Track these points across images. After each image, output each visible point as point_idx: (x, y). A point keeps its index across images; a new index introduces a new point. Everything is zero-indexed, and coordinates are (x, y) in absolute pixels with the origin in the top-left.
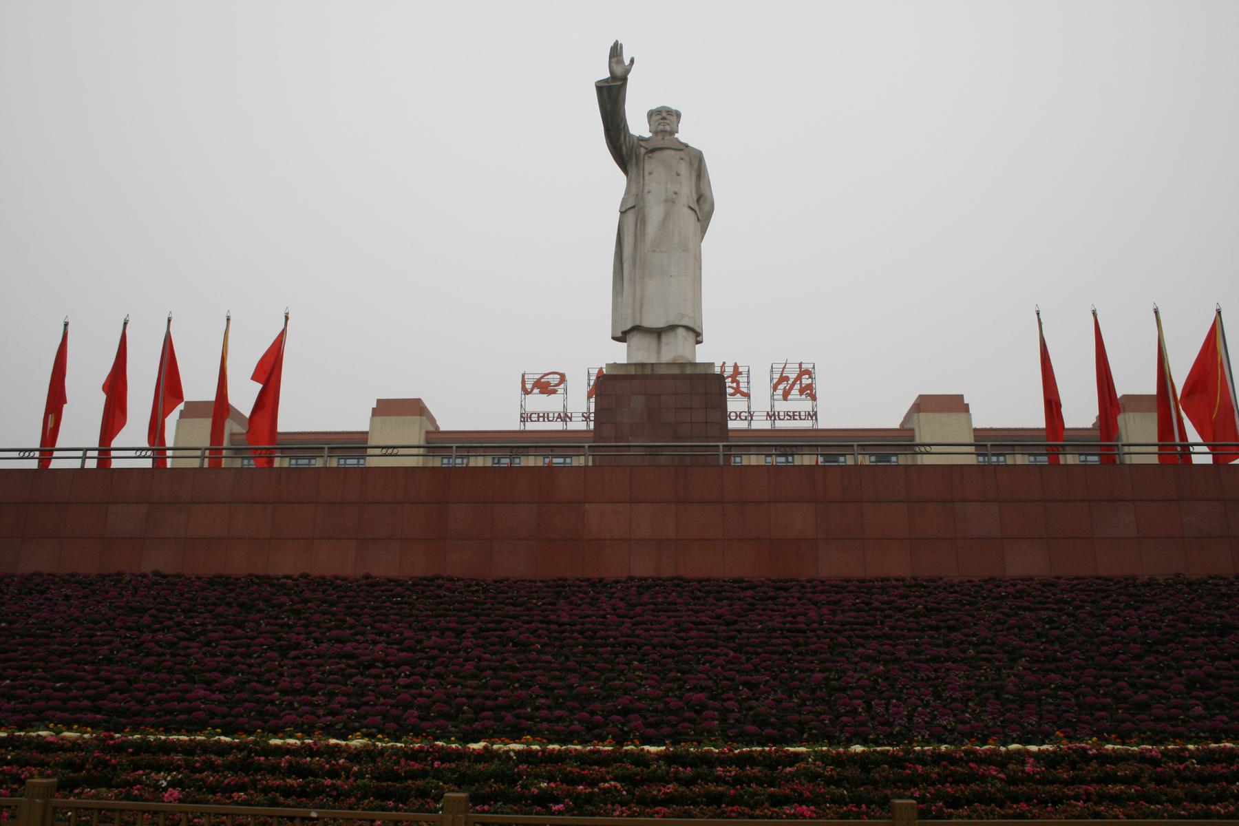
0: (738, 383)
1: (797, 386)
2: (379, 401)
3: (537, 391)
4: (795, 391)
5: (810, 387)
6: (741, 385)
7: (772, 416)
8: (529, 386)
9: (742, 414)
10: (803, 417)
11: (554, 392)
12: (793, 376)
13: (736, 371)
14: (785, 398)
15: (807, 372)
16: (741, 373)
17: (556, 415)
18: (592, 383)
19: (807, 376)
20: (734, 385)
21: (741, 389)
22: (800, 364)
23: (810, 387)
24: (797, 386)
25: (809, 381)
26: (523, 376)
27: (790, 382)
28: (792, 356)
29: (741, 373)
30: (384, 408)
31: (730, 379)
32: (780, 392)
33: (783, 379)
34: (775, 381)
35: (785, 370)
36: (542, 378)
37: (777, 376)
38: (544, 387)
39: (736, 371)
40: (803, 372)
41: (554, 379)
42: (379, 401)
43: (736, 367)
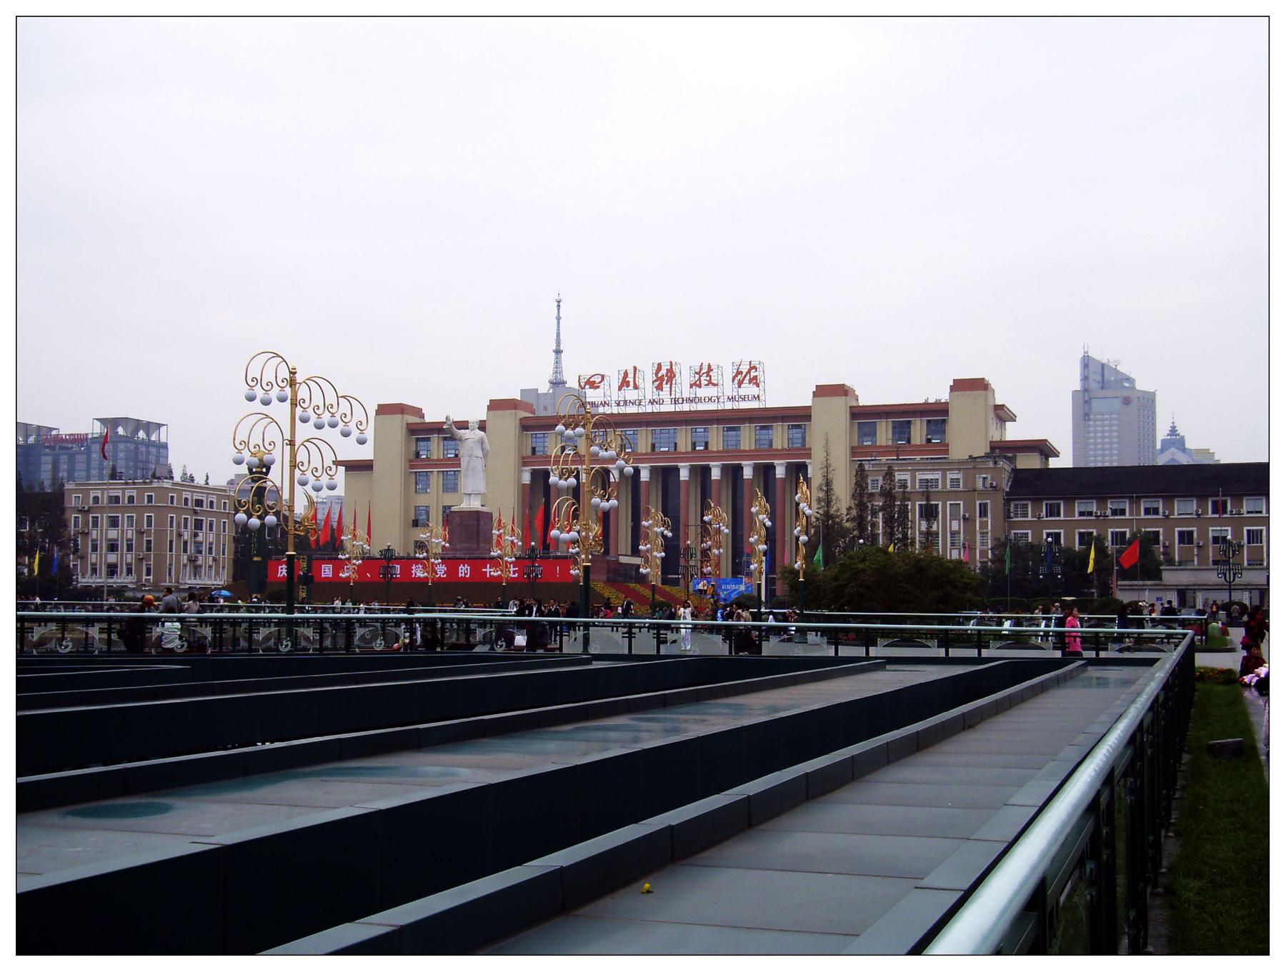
0: (710, 377)
1: (748, 378)
2: (490, 401)
3: (587, 387)
4: (746, 381)
5: (755, 377)
6: (712, 378)
7: (732, 399)
8: (582, 384)
9: (713, 398)
10: (750, 399)
11: (598, 387)
12: (745, 371)
13: (710, 369)
14: (740, 384)
15: (755, 368)
16: (712, 370)
18: (620, 381)
19: (754, 370)
20: (708, 378)
21: (712, 381)
22: (750, 362)
23: (755, 377)
24: (748, 378)
25: (756, 374)
26: (579, 376)
27: (743, 375)
28: (745, 357)
29: (712, 370)
31: (705, 375)
32: (736, 381)
33: (739, 373)
34: (734, 374)
35: (740, 367)
36: (590, 378)
37: (735, 371)
38: (592, 385)
39: (710, 369)
40: (753, 368)
41: (598, 379)
42: (490, 401)
43: (709, 366)
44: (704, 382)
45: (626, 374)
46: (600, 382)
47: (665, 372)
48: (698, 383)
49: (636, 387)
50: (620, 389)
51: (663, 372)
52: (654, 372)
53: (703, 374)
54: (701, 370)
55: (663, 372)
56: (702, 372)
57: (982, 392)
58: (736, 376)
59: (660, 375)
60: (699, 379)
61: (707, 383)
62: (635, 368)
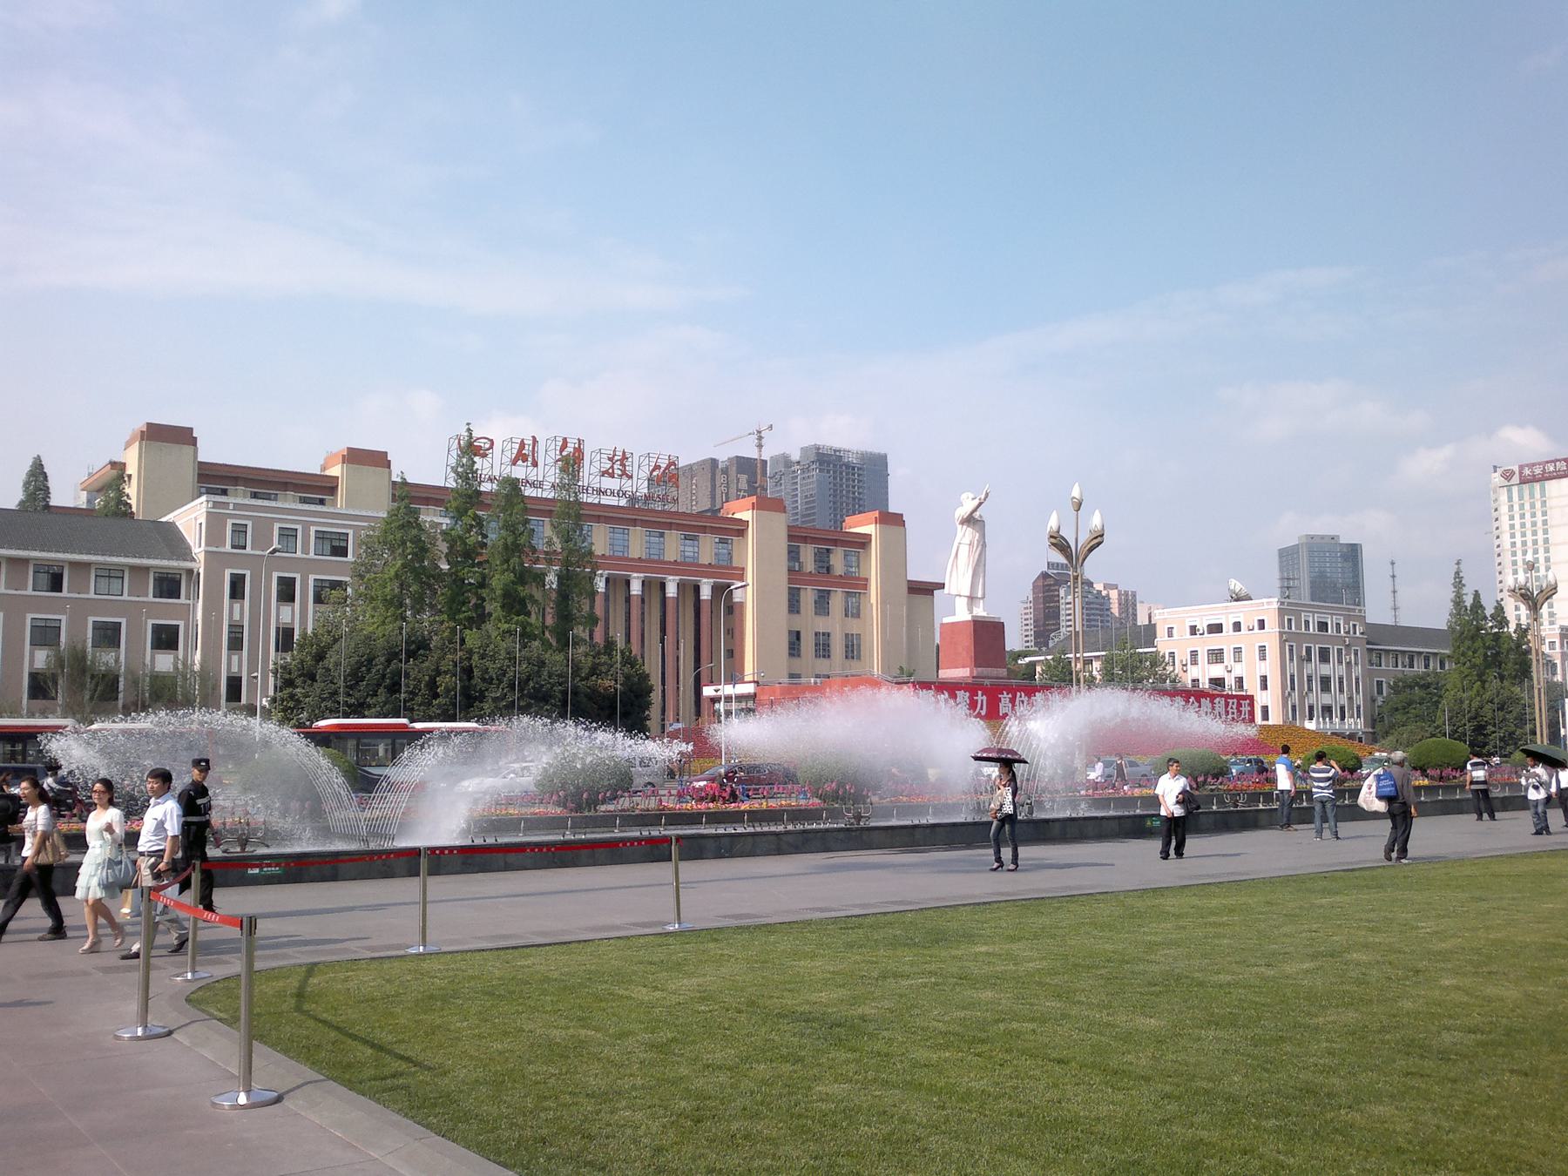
0: (624, 466)
12: (663, 466)
13: (624, 457)
17: (487, 477)
30: (356, 457)
31: (619, 463)
34: (651, 468)
39: (624, 457)
43: (624, 453)
44: (618, 472)
45: (522, 445)
46: (488, 449)
47: (572, 450)
48: (610, 471)
49: (535, 464)
50: (514, 463)
51: (570, 449)
52: (558, 448)
53: (617, 461)
54: (615, 455)
55: (570, 449)
56: (616, 458)
57: (896, 529)
58: (654, 470)
59: (564, 453)
60: (612, 467)
61: (620, 472)
62: (534, 438)
